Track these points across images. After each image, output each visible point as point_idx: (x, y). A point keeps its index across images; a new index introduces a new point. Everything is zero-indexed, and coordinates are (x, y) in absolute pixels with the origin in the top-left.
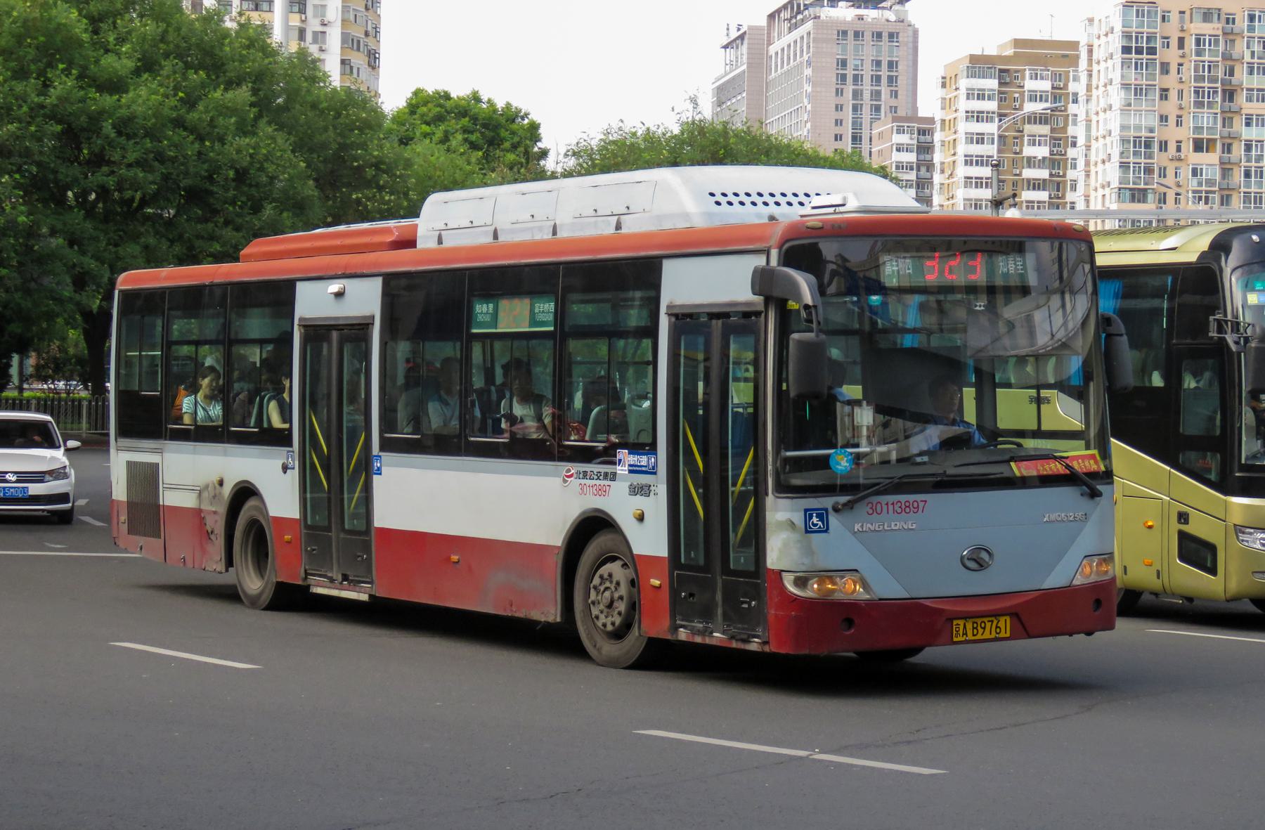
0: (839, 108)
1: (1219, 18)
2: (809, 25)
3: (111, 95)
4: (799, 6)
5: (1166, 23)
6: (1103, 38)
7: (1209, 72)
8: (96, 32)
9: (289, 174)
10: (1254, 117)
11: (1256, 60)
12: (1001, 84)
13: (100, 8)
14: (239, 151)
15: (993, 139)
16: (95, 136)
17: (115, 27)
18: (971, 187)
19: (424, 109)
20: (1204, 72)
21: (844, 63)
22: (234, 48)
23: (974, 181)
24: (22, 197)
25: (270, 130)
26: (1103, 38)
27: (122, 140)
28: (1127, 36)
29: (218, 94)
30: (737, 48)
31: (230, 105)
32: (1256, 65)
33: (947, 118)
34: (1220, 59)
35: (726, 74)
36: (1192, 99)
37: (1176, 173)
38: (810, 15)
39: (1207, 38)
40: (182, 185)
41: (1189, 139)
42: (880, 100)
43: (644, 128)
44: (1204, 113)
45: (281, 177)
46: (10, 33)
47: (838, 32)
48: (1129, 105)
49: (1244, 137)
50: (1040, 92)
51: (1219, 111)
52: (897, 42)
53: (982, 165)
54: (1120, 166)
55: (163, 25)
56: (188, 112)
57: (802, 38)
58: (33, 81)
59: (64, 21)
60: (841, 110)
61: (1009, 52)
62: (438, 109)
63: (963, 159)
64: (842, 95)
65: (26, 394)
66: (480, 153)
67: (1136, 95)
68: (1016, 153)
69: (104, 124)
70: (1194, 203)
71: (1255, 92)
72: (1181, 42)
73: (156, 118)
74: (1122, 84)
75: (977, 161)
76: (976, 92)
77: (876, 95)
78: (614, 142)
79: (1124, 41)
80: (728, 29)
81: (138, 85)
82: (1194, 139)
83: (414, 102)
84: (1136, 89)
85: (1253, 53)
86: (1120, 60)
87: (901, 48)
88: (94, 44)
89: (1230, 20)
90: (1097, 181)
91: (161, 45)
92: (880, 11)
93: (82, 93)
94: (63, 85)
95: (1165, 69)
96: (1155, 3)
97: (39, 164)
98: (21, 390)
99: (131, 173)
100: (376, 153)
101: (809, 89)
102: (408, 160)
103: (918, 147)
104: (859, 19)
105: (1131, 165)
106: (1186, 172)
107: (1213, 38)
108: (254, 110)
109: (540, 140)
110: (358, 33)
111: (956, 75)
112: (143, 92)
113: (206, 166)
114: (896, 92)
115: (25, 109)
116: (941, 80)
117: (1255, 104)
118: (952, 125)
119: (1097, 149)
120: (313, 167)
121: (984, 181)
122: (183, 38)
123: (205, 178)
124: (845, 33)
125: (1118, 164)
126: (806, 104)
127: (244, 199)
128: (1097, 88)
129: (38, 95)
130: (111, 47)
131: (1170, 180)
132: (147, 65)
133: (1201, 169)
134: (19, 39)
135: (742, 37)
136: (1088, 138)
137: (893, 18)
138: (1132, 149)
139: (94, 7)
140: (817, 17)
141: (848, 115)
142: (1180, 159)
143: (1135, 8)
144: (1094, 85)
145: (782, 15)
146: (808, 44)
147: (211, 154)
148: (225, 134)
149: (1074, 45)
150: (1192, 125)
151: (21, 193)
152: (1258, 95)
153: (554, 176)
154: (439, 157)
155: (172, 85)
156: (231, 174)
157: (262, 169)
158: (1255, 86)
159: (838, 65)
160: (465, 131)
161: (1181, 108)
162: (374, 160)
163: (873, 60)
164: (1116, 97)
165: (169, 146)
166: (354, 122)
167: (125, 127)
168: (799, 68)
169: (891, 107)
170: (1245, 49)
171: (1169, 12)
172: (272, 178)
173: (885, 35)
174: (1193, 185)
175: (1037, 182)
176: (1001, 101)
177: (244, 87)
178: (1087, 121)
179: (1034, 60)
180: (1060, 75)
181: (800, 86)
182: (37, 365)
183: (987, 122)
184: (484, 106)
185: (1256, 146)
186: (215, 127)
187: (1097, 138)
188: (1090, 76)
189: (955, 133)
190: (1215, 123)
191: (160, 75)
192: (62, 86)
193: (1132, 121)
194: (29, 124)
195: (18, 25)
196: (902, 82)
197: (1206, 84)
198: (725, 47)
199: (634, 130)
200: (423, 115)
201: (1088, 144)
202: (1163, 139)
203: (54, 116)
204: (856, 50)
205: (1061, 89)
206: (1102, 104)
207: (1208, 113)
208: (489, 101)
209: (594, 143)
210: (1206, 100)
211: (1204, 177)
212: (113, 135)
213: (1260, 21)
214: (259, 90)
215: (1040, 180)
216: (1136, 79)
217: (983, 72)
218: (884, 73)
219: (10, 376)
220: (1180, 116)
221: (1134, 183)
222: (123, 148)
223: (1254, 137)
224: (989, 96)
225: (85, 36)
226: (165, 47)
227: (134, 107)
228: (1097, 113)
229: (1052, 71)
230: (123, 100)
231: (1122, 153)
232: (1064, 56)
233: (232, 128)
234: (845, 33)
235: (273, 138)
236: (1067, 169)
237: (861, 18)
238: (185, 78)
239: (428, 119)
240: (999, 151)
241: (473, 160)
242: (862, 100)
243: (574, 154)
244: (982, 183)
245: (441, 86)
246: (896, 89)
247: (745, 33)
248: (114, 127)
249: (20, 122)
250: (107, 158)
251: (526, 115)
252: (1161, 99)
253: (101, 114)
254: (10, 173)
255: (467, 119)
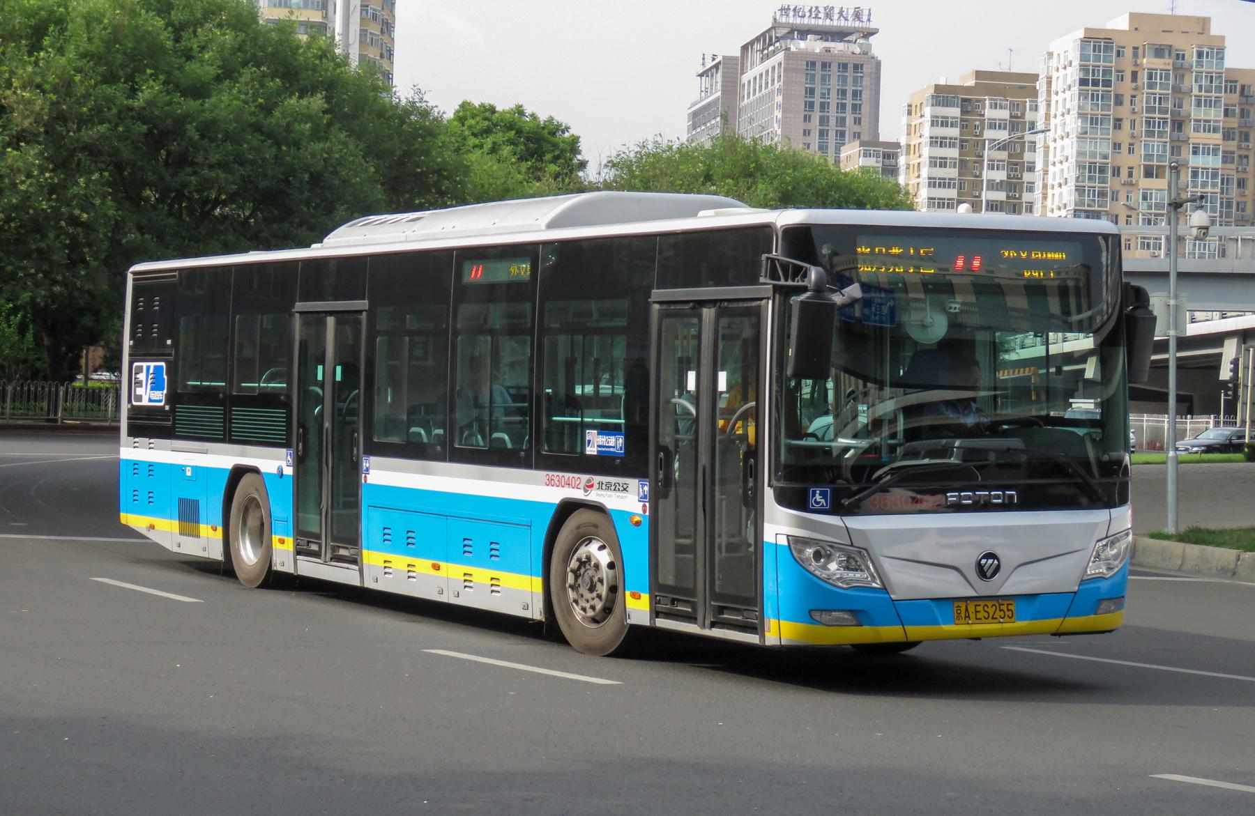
0: (807, 133)
1: (1170, 55)
2: (780, 56)
3: (195, 100)
4: (771, 38)
5: (1121, 58)
6: (1061, 70)
7: (1160, 103)
8: (177, 40)
9: (360, 178)
10: (1201, 146)
11: (1203, 93)
12: (963, 112)
13: (182, 17)
14: (313, 156)
15: (955, 163)
16: (179, 138)
17: (196, 36)
18: (934, 207)
19: (471, 122)
20: (1155, 103)
21: (811, 92)
22: (308, 58)
23: (936, 201)
24: (110, 194)
25: (342, 136)
26: (1061, 70)
27: (205, 142)
28: (1084, 69)
29: (293, 101)
30: (712, 76)
31: (305, 111)
32: (1203, 99)
33: (912, 144)
34: (1170, 91)
35: (702, 100)
36: (1144, 129)
37: (1128, 196)
38: (781, 47)
39: (1159, 72)
40: (260, 186)
41: (1140, 166)
42: (845, 126)
43: (677, 142)
44: (1154, 141)
45: (353, 181)
46: (101, 39)
47: (807, 63)
48: (1086, 133)
49: (1191, 164)
50: (999, 120)
51: (1168, 140)
52: (861, 73)
53: (944, 187)
54: (1076, 190)
55: (242, 35)
56: (265, 118)
57: (773, 68)
58: (121, 85)
59: (150, 29)
60: (809, 135)
61: (971, 82)
62: (486, 123)
63: (927, 181)
64: (810, 121)
65: (90, 384)
66: (529, 163)
67: (1091, 124)
68: (977, 177)
69: (188, 127)
70: (1144, 224)
71: (1202, 123)
72: (1134, 76)
73: (236, 122)
74: (1079, 114)
75: (940, 184)
76: (940, 120)
77: (842, 121)
78: (648, 155)
79: (1082, 73)
80: (704, 59)
81: (221, 91)
82: (1145, 166)
83: (461, 114)
84: (1092, 119)
85: (1200, 87)
86: (1077, 92)
87: (865, 79)
88: (175, 52)
89: (1181, 57)
90: (1053, 204)
91: (239, 54)
92: (846, 44)
93: (168, 98)
94: (149, 91)
95: (1119, 100)
96: (1110, 39)
97: (119, 167)
98: (87, 379)
99: (213, 174)
100: (439, 160)
101: (780, 115)
102: (467, 167)
103: (883, 169)
104: (826, 51)
105: (1087, 189)
106: (1137, 197)
107: (1164, 72)
108: (328, 116)
109: (580, 154)
110: (373, 53)
111: (921, 104)
112: (225, 98)
113: (282, 169)
114: (860, 119)
115: (114, 111)
116: (906, 108)
117: (1202, 134)
118: (917, 150)
119: (1054, 174)
120: (381, 172)
121: (946, 201)
122: (260, 47)
123: (282, 180)
124: (813, 64)
125: (1073, 188)
126: (776, 128)
127: (318, 201)
128: (1055, 117)
129: (127, 98)
130: (195, 54)
131: (1122, 201)
132: (228, 73)
133: (1151, 193)
134: (109, 43)
135: (716, 67)
136: (1046, 163)
137: (858, 50)
138: (1087, 174)
139: (177, 16)
140: (788, 49)
141: (815, 140)
142: (1131, 184)
143: (1092, 44)
144: (1052, 112)
145: (755, 47)
146: (779, 73)
147: (288, 158)
148: (300, 140)
149: (1035, 77)
150: (1143, 153)
151: (111, 190)
152: (1205, 126)
153: (592, 188)
154: (491, 165)
155: (251, 92)
156: (306, 177)
157: (335, 173)
158: (1202, 117)
159: (806, 93)
160: (511, 142)
161: (1133, 136)
162: (436, 167)
163: (838, 90)
164: (1073, 124)
165: (250, 150)
166: (416, 129)
167: (207, 130)
168: (770, 96)
169: (855, 133)
170: (1194, 83)
171: (1124, 48)
172: (345, 182)
173: (850, 67)
174: (1143, 207)
175: (994, 204)
176: (962, 127)
177: (319, 95)
178: (1045, 148)
179: (993, 91)
180: (1018, 105)
181: (771, 110)
182: (105, 356)
183: (950, 147)
184: (528, 119)
185: (1203, 172)
186: (292, 132)
187: (1054, 163)
188: (1049, 106)
189: (920, 157)
190: (1165, 151)
191: (238, 82)
192: (149, 91)
193: (1088, 148)
194: (117, 125)
195: (108, 31)
196: (866, 109)
197: (1157, 115)
198: (701, 75)
199: (670, 144)
200: (470, 127)
201: (1046, 169)
202: (1117, 164)
203: (141, 117)
204: (823, 78)
205: (1018, 117)
206: (1060, 132)
207: (1158, 142)
208: (533, 116)
209: (632, 155)
210: (1156, 129)
211: (1153, 201)
212: (197, 137)
213: (1207, 57)
214: (332, 98)
215: (997, 201)
216: (1092, 110)
217: (947, 100)
218: (849, 101)
219: (81, 367)
220: (1131, 144)
221: (1089, 205)
222: (205, 150)
223: (1200, 165)
224: (952, 123)
225: (169, 44)
226: (242, 56)
227: (217, 111)
228: (1055, 140)
229: (1010, 101)
230: (207, 105)
231: (1078, 177)
232: (1022, 87)
233: (307, 133)
234: (813, 64)
235: (345, 144)
236: (1022, 192)
237: (828, 50)
238: (262, 86)
239: (475, 131)
240: (960, 174)
241: (523, 170)
242: (828, 126)
243: (614, 165)
244: (944, 203)
245: (488, 101)
246: (859, 116)
247: (720, 62)
248: (197, 130)
249: (110, 123)
250: (190, 159)
251: (567, 129)
252: (1115, 128)
253: (187, 117)
254: (101, 171)
255: (513, 133)
